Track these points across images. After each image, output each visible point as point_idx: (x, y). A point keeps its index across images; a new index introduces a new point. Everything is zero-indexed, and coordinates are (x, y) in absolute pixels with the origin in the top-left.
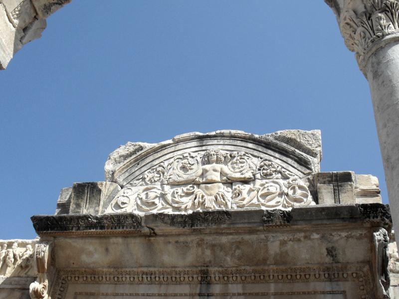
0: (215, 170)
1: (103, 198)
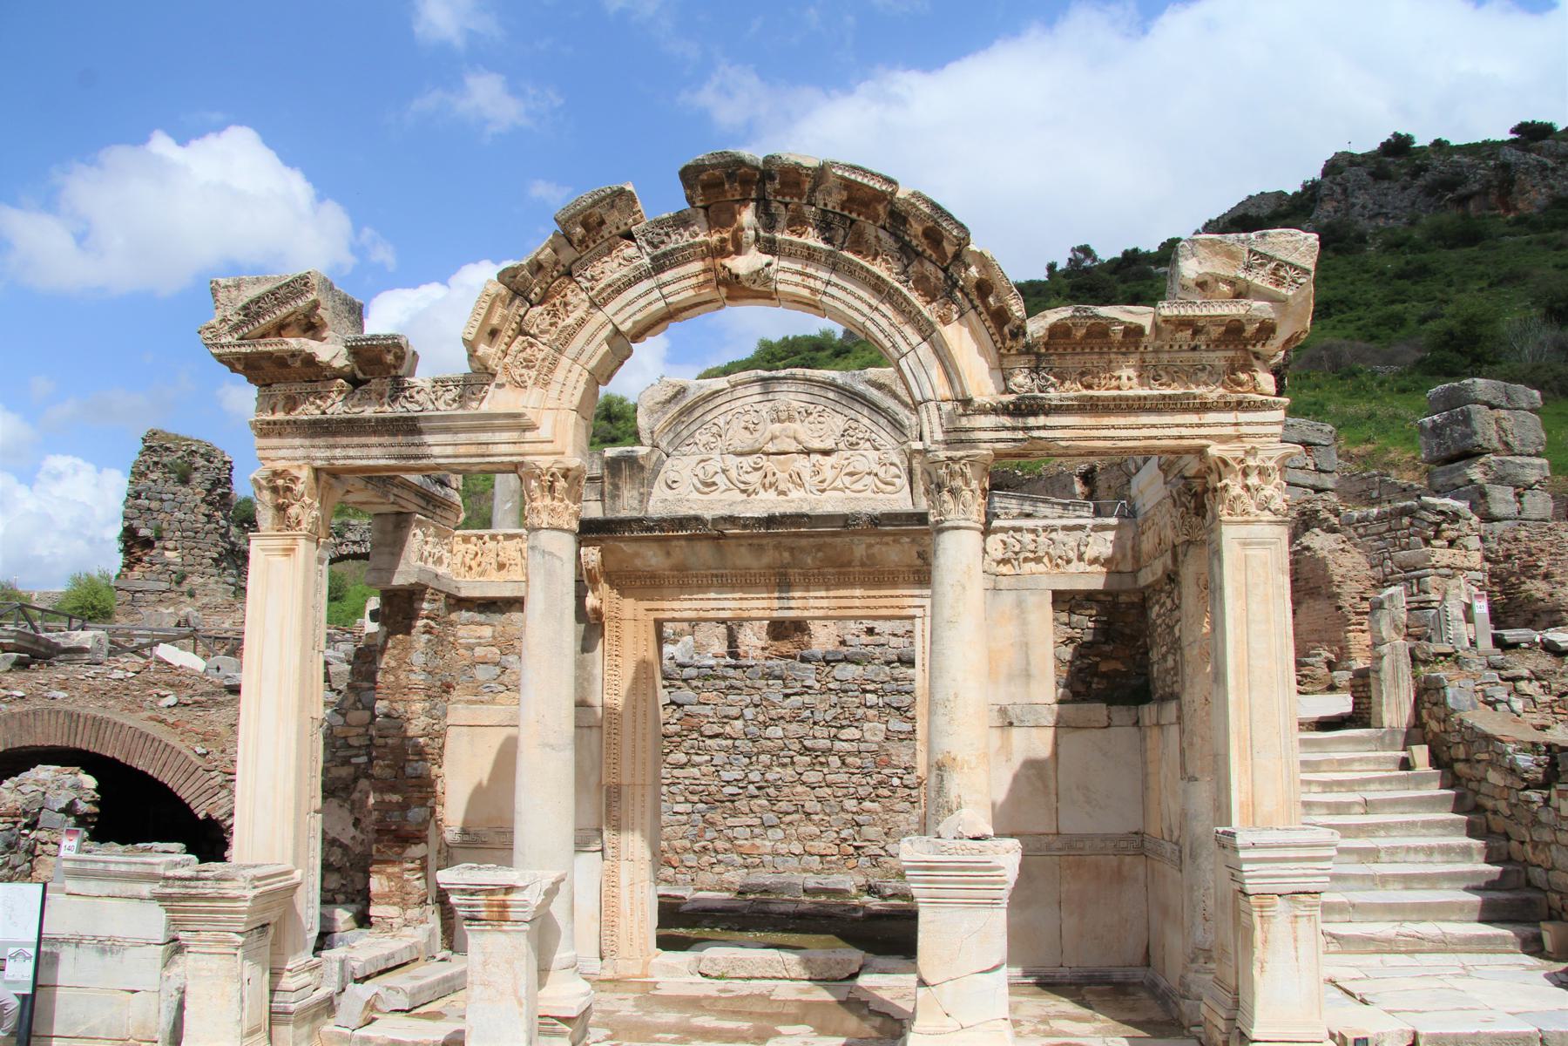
1: (646, 474)
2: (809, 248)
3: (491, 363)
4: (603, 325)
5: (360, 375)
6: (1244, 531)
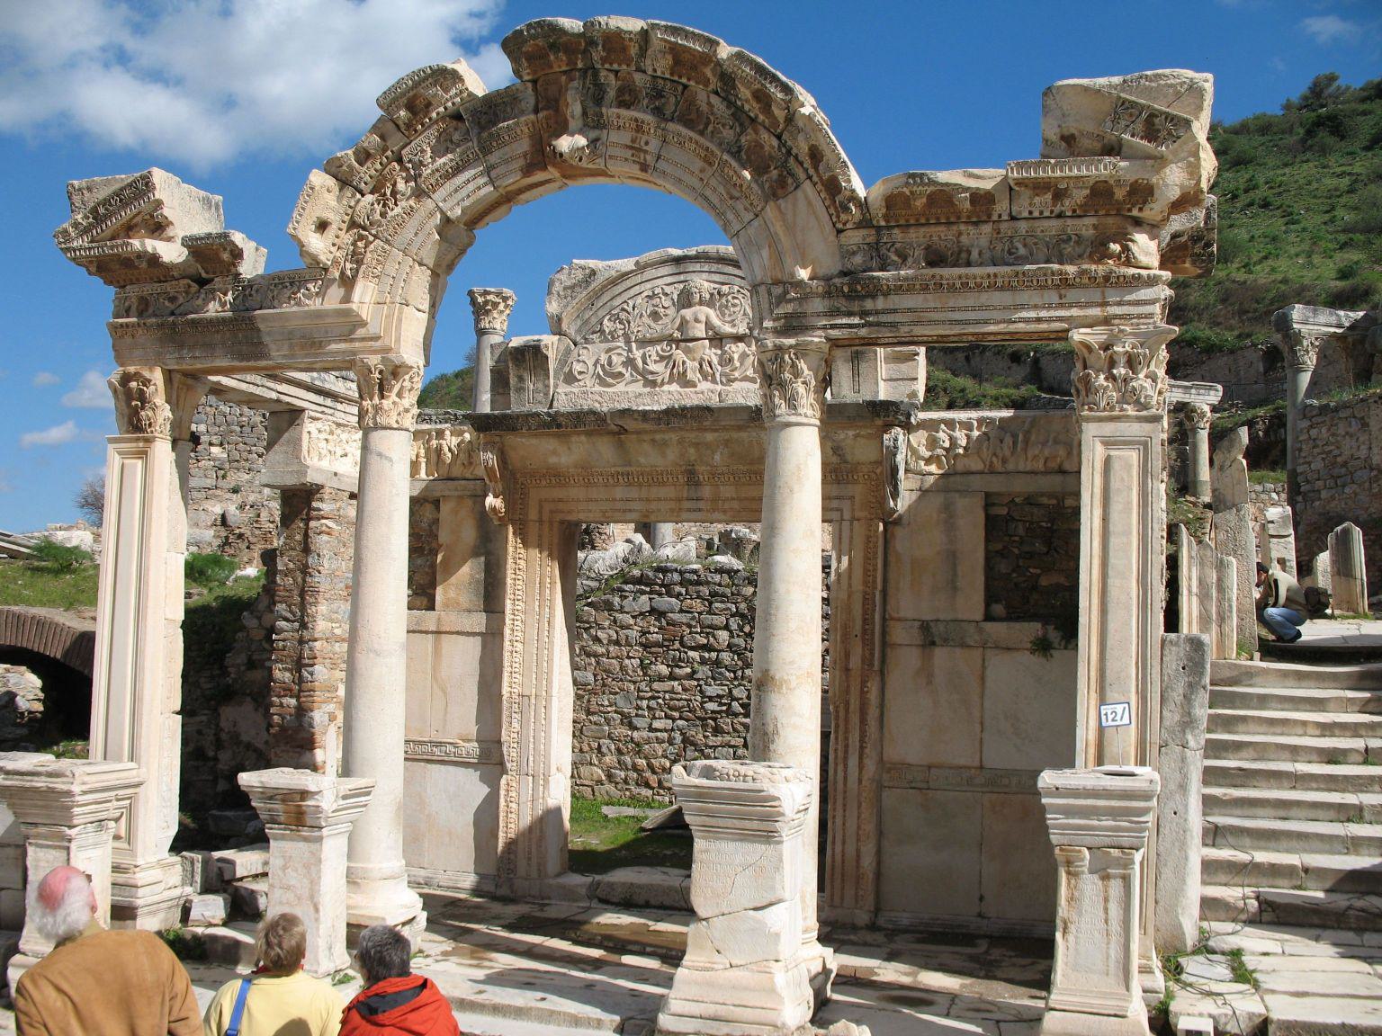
0: (697, 320)
2: (636, 120)
3: (323, 258)
4: (432, 214)
5: (204, 275)
6: (1109, 429)
